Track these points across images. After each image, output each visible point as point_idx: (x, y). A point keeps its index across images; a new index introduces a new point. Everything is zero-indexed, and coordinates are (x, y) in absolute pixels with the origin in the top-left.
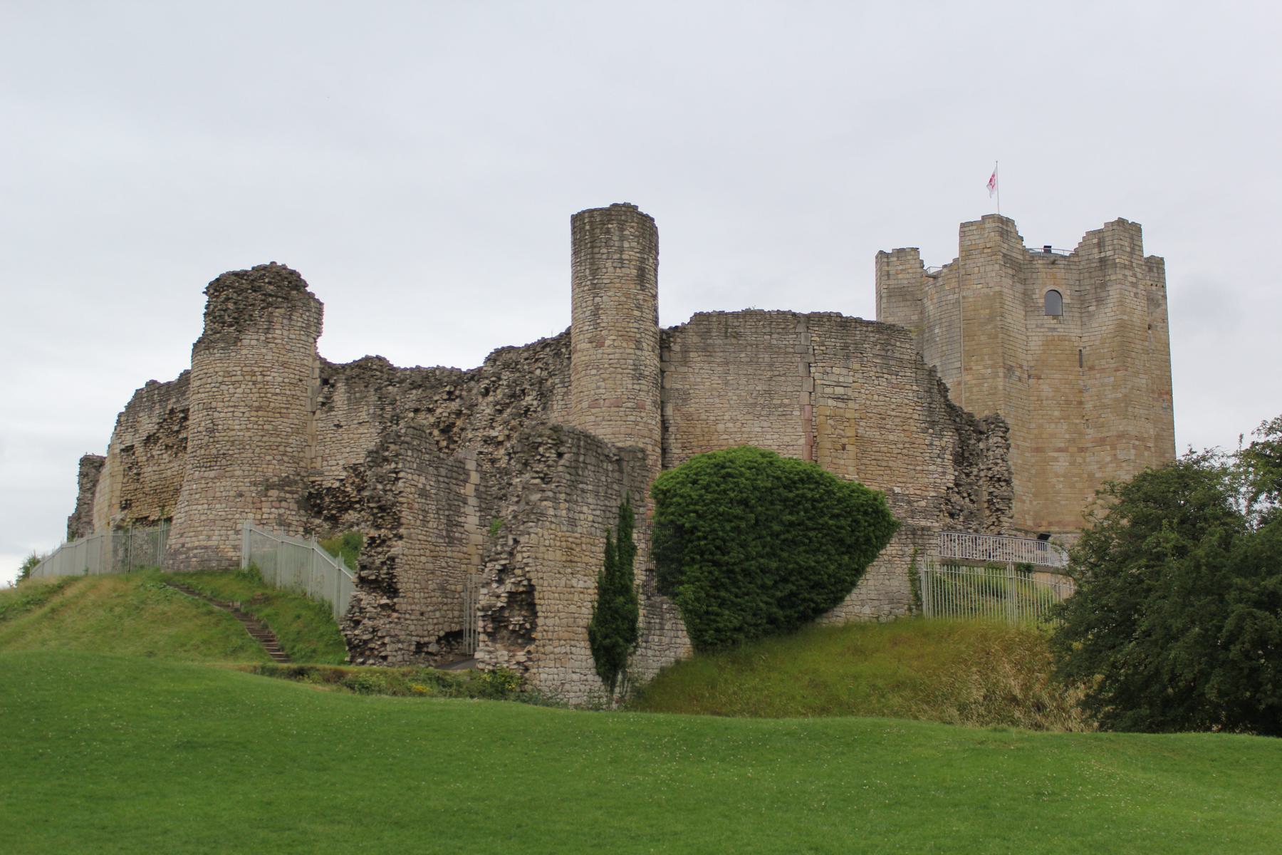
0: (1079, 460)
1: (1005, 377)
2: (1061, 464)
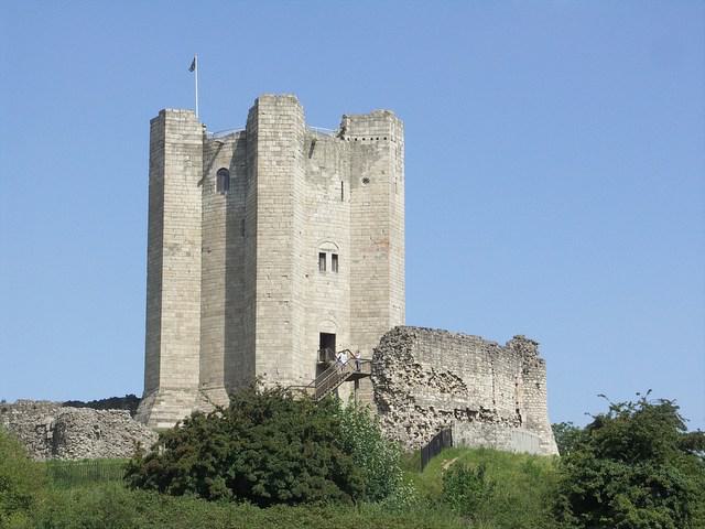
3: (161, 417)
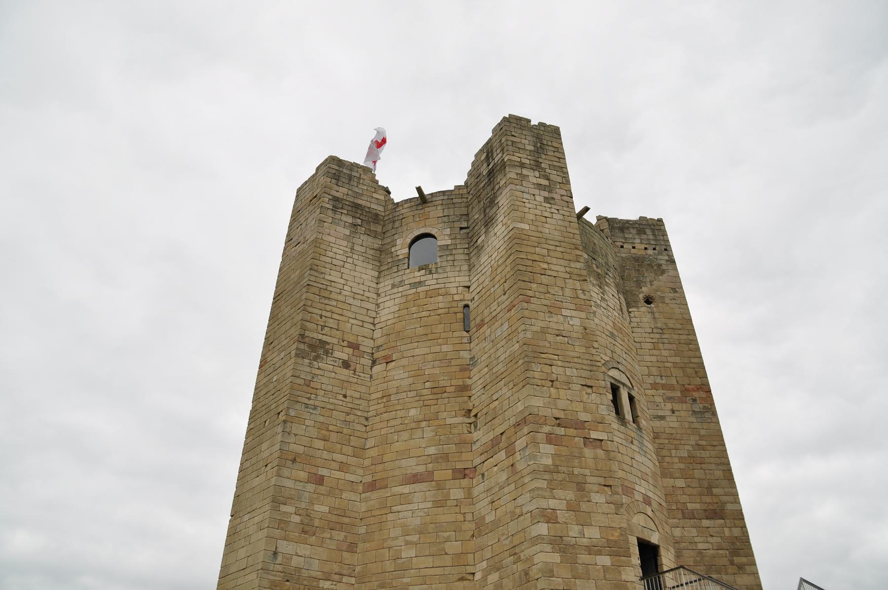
0: (457, 494)
1: (300, 355)
2: (417, 505)
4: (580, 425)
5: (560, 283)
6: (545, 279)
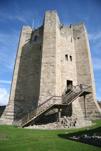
0: (36, 76)
3: (8, 111)
4: (49, 63)
5: (51, 40)
6: (48, 40)
